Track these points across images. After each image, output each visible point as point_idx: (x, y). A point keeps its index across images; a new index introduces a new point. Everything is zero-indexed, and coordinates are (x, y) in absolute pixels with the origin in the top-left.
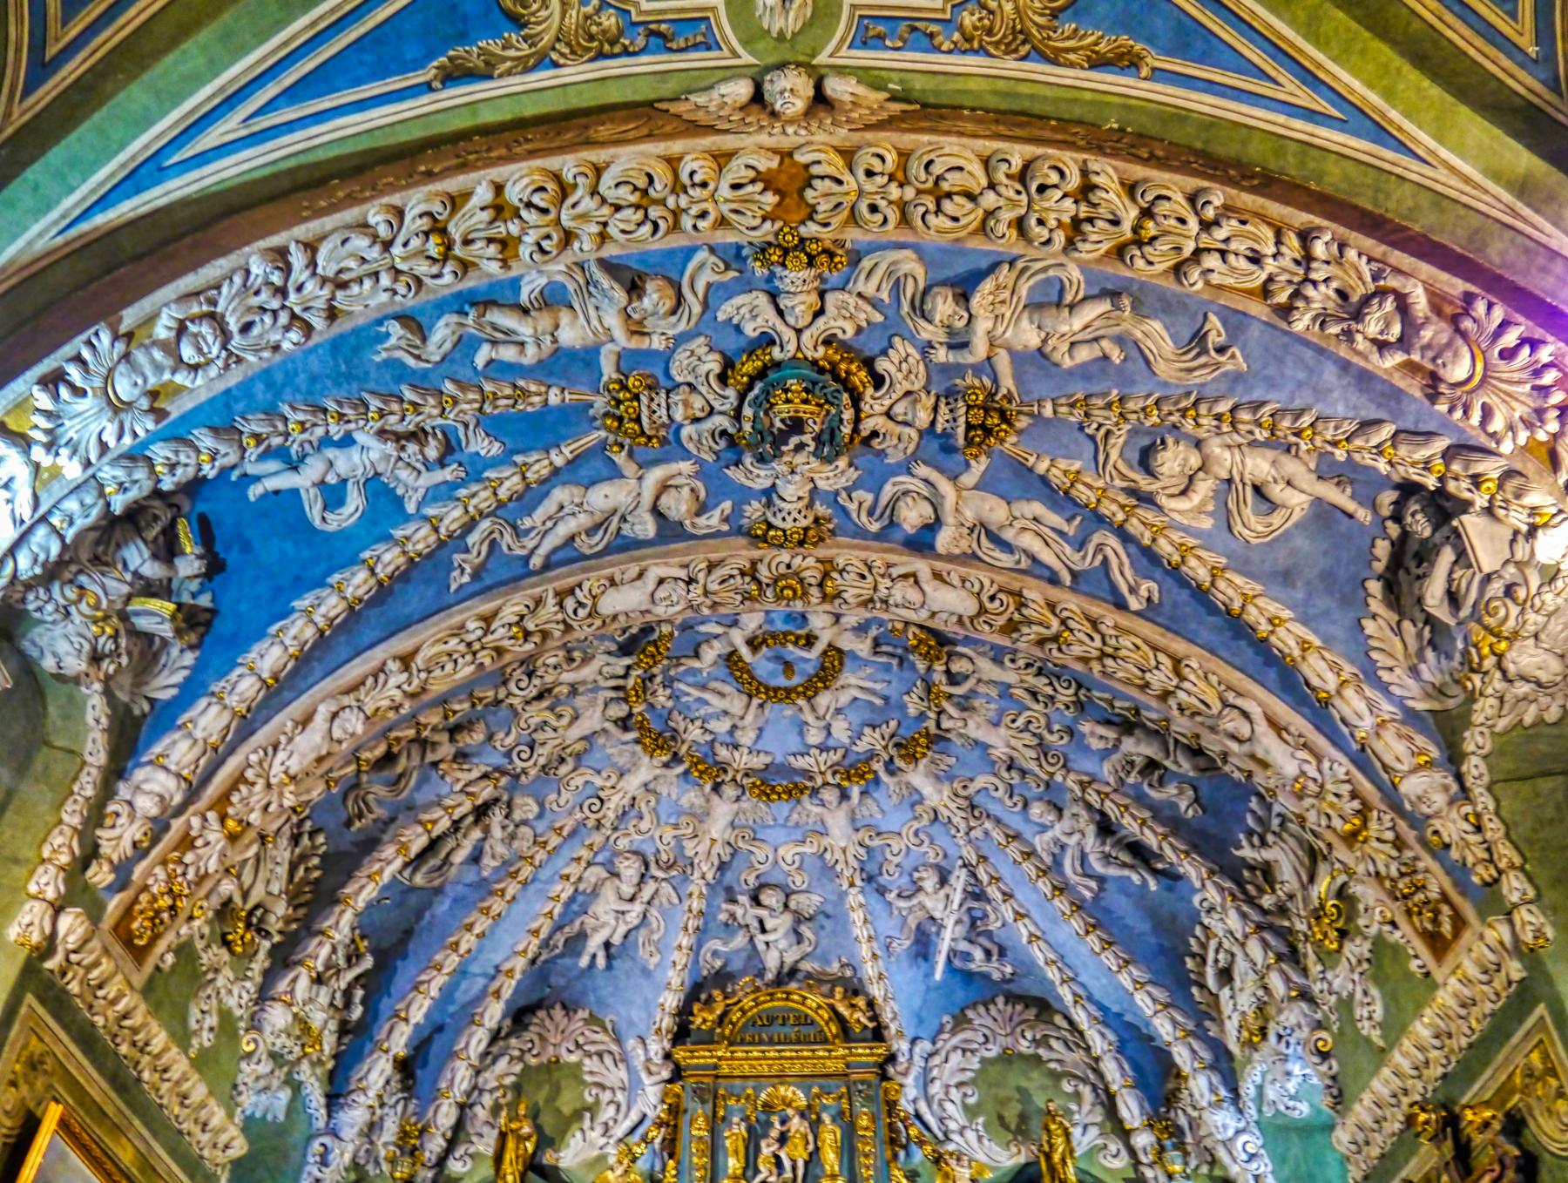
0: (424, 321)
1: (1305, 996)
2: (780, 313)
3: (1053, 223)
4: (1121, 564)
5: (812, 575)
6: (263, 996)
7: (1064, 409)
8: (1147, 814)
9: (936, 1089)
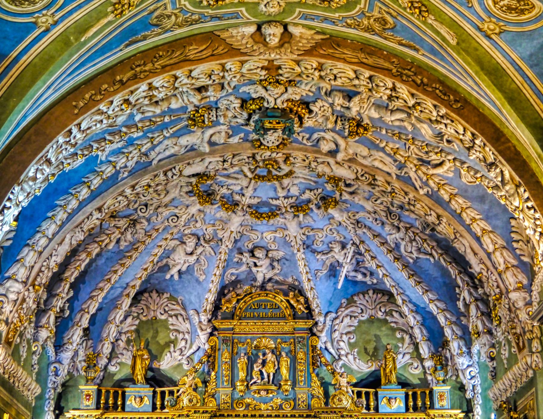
6: (37, 327)
8: (434, 244)
9: (336, 335)
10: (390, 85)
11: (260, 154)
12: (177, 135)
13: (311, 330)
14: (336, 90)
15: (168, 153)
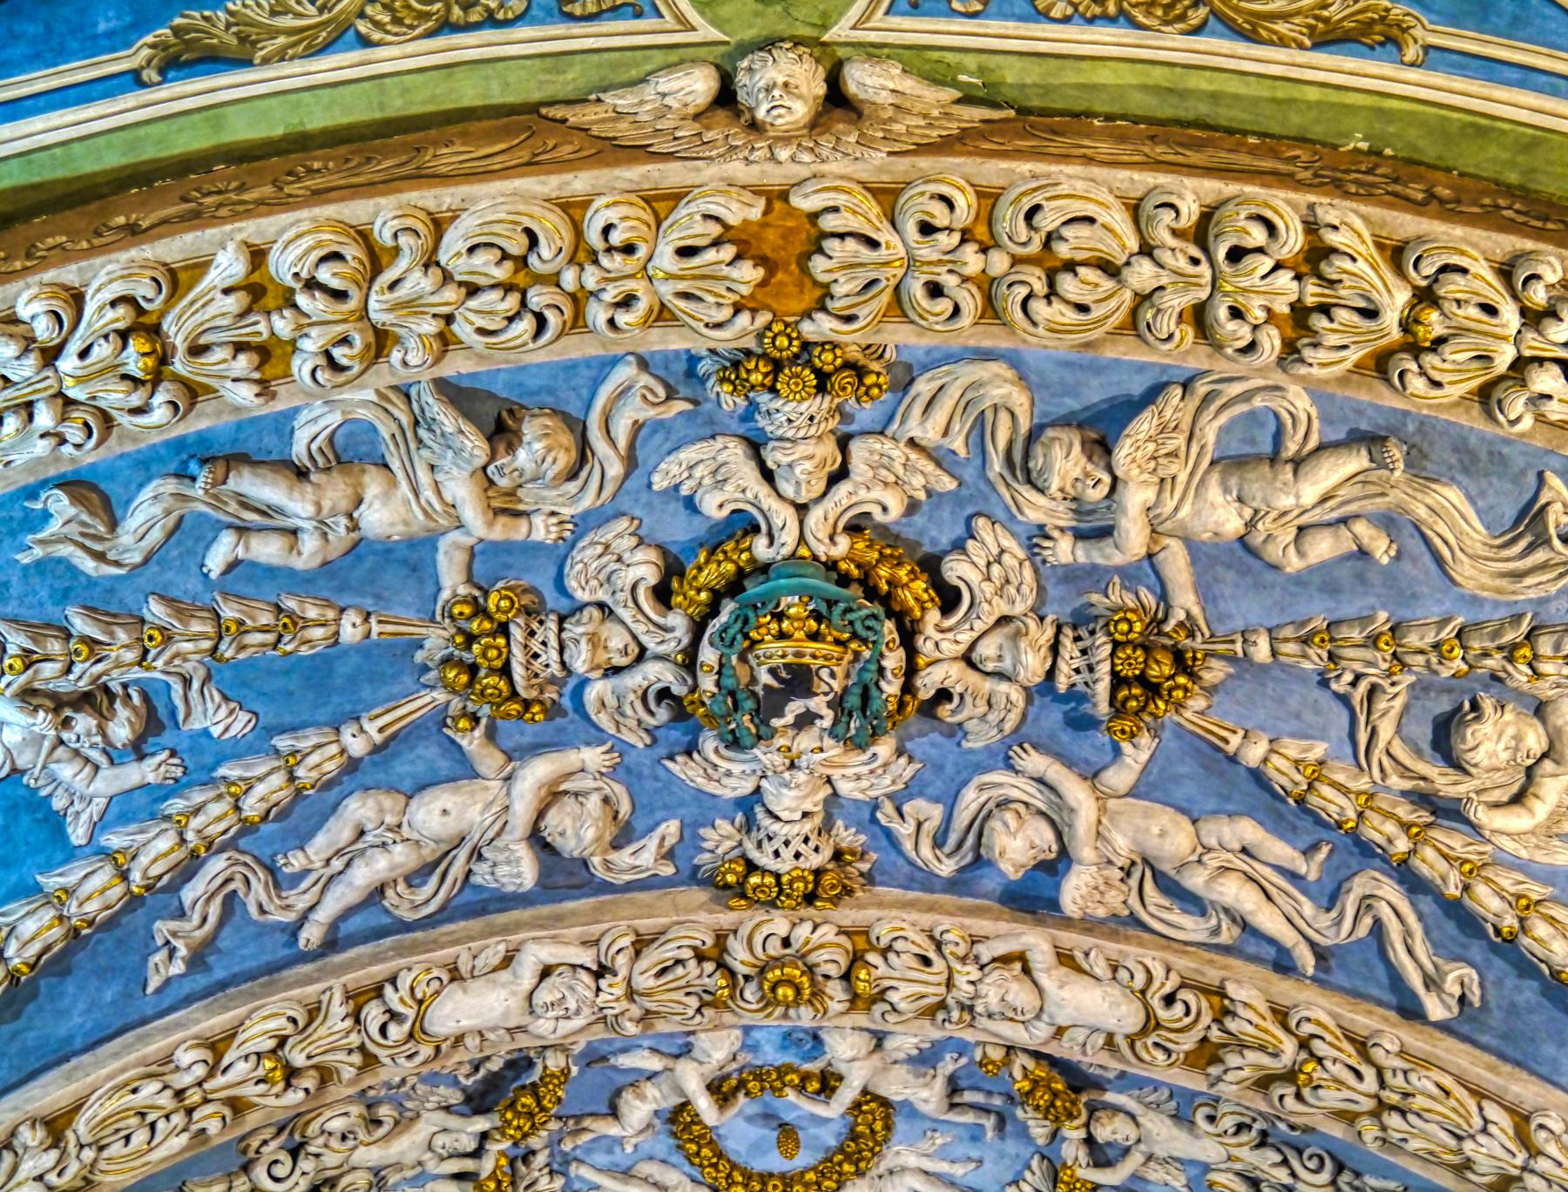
0: (113, 489)
2: (768, 476)
3: (1261, 315)
4: (1407, 934)
5: (830, 961)
7: (1291, 648)
11: (744, 932)
14: (1053, 424)
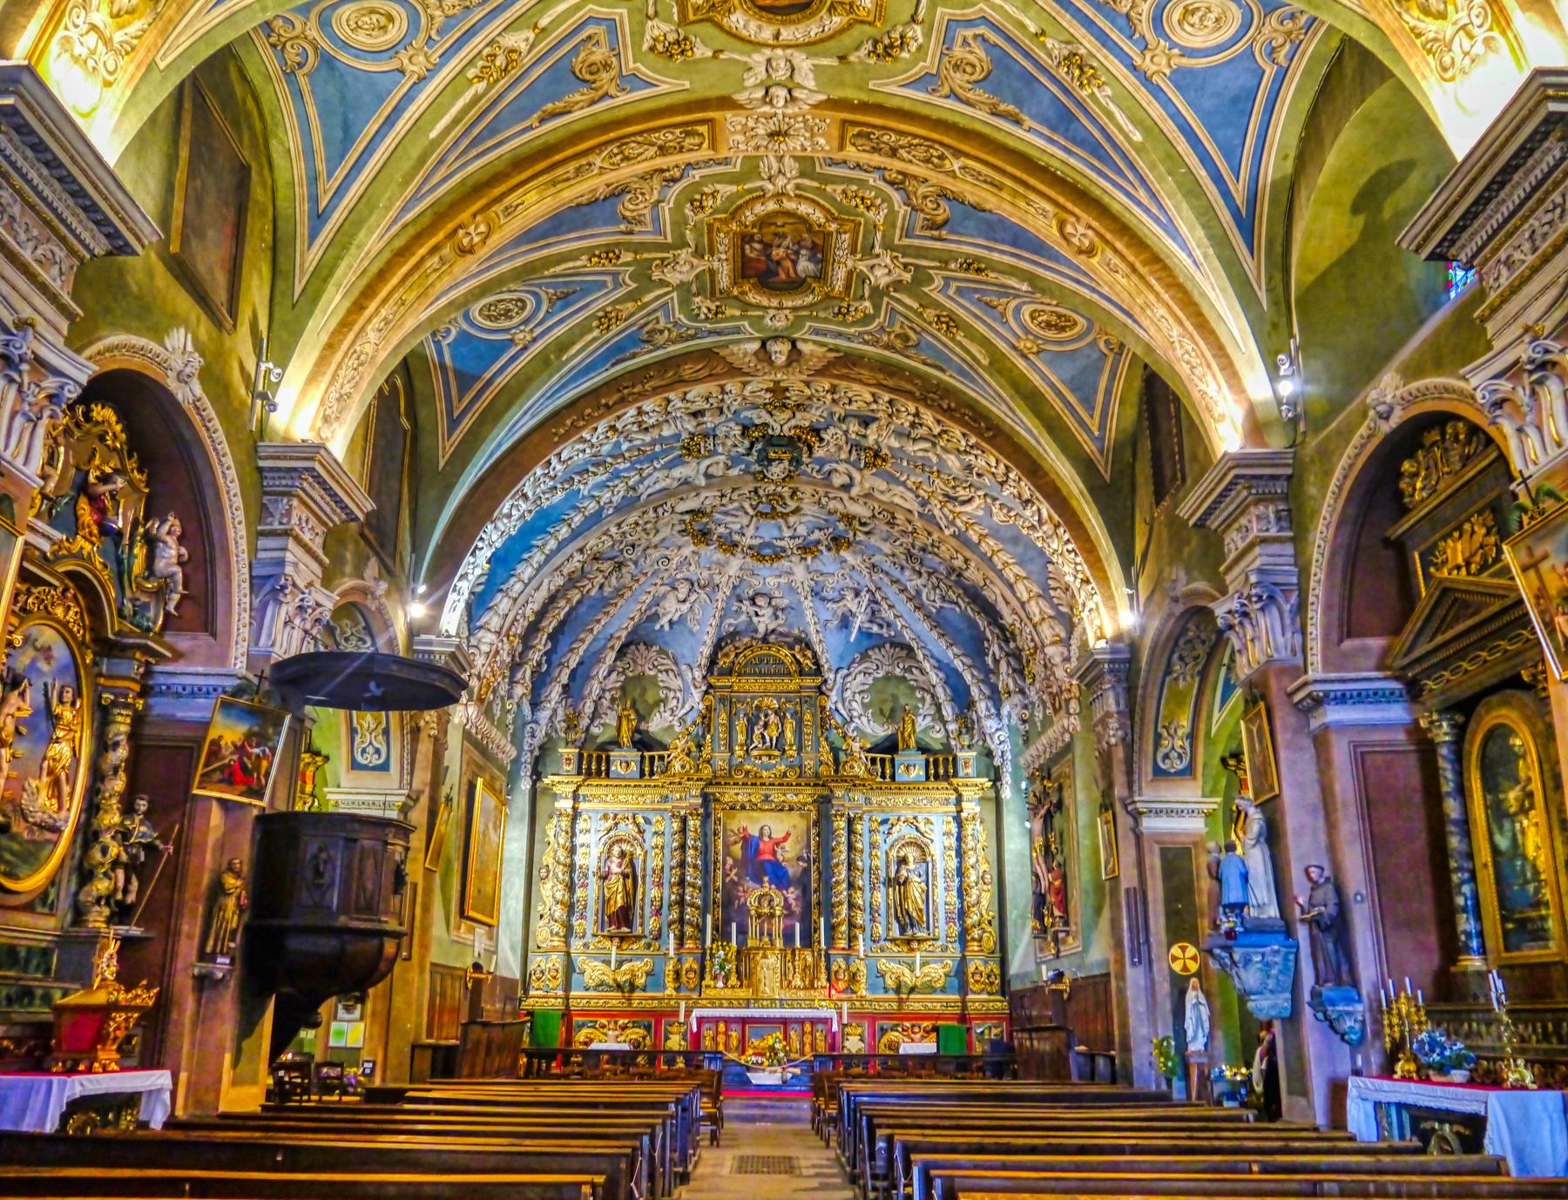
1: (1022, 692)
6: (512, 683)
9: (848, 694)
10: (912, 410)
12: (670, 466)
13: (819, 688)
15: (658, 487)
